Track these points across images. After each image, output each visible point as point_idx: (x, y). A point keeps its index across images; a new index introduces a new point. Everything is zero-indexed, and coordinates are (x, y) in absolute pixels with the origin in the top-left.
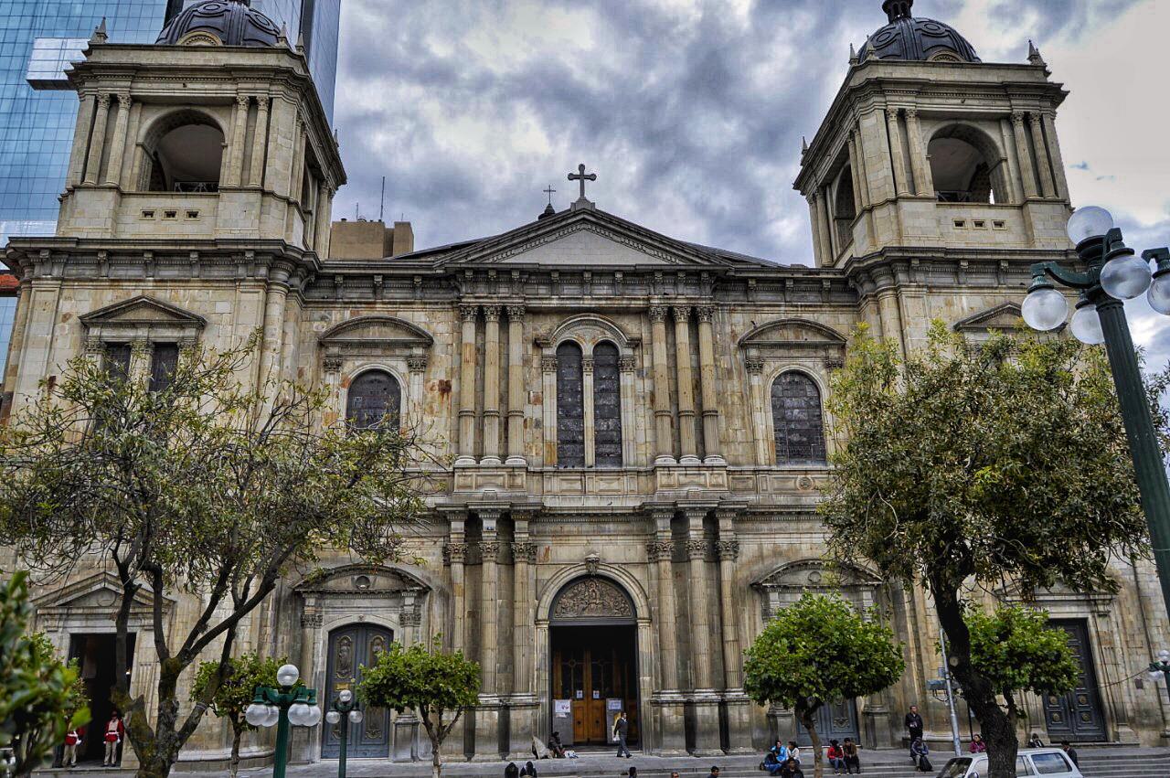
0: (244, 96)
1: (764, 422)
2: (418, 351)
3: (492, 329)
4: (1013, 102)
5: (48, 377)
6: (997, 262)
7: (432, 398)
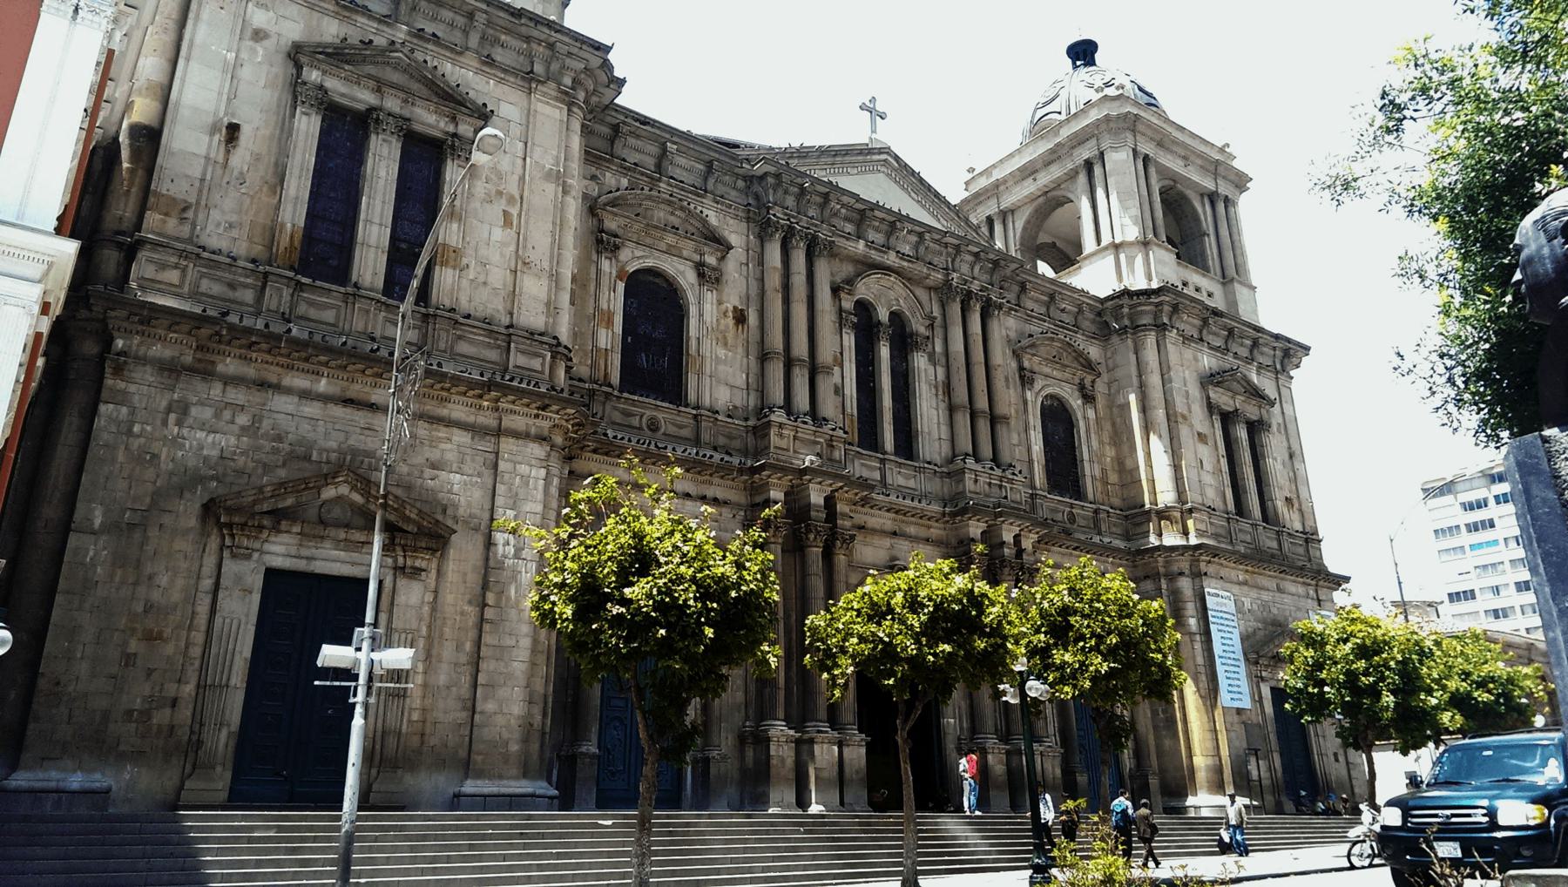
5: (226, 121)
7: (727, 326)
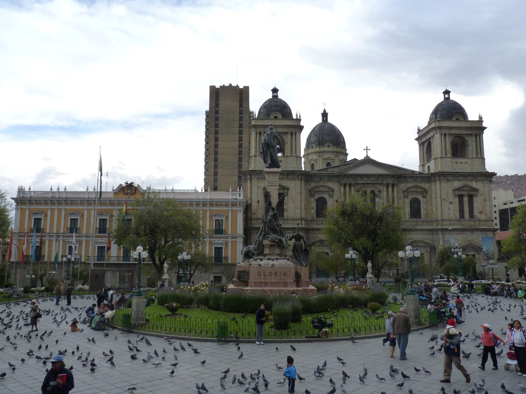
0: (290, 132)
1: (408, 210)
2: (331, 193)
3: (347, 188)
4: (473, 131)
6: (464, 175)
